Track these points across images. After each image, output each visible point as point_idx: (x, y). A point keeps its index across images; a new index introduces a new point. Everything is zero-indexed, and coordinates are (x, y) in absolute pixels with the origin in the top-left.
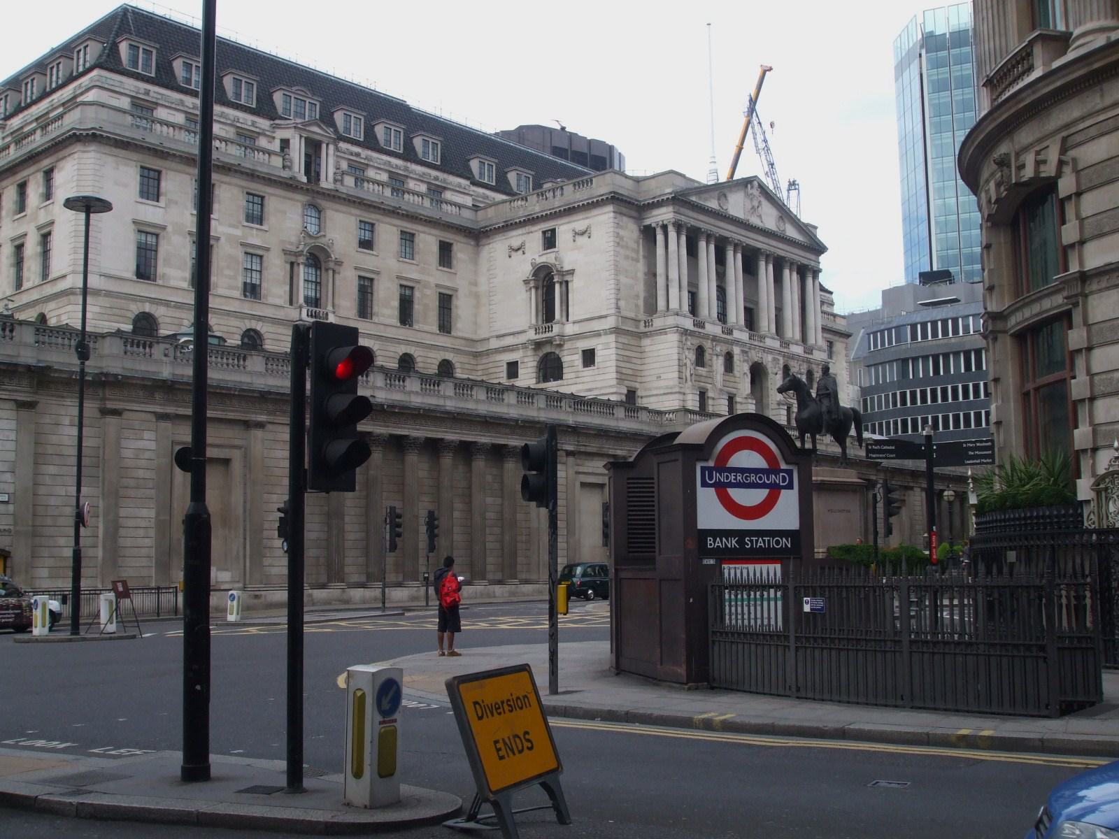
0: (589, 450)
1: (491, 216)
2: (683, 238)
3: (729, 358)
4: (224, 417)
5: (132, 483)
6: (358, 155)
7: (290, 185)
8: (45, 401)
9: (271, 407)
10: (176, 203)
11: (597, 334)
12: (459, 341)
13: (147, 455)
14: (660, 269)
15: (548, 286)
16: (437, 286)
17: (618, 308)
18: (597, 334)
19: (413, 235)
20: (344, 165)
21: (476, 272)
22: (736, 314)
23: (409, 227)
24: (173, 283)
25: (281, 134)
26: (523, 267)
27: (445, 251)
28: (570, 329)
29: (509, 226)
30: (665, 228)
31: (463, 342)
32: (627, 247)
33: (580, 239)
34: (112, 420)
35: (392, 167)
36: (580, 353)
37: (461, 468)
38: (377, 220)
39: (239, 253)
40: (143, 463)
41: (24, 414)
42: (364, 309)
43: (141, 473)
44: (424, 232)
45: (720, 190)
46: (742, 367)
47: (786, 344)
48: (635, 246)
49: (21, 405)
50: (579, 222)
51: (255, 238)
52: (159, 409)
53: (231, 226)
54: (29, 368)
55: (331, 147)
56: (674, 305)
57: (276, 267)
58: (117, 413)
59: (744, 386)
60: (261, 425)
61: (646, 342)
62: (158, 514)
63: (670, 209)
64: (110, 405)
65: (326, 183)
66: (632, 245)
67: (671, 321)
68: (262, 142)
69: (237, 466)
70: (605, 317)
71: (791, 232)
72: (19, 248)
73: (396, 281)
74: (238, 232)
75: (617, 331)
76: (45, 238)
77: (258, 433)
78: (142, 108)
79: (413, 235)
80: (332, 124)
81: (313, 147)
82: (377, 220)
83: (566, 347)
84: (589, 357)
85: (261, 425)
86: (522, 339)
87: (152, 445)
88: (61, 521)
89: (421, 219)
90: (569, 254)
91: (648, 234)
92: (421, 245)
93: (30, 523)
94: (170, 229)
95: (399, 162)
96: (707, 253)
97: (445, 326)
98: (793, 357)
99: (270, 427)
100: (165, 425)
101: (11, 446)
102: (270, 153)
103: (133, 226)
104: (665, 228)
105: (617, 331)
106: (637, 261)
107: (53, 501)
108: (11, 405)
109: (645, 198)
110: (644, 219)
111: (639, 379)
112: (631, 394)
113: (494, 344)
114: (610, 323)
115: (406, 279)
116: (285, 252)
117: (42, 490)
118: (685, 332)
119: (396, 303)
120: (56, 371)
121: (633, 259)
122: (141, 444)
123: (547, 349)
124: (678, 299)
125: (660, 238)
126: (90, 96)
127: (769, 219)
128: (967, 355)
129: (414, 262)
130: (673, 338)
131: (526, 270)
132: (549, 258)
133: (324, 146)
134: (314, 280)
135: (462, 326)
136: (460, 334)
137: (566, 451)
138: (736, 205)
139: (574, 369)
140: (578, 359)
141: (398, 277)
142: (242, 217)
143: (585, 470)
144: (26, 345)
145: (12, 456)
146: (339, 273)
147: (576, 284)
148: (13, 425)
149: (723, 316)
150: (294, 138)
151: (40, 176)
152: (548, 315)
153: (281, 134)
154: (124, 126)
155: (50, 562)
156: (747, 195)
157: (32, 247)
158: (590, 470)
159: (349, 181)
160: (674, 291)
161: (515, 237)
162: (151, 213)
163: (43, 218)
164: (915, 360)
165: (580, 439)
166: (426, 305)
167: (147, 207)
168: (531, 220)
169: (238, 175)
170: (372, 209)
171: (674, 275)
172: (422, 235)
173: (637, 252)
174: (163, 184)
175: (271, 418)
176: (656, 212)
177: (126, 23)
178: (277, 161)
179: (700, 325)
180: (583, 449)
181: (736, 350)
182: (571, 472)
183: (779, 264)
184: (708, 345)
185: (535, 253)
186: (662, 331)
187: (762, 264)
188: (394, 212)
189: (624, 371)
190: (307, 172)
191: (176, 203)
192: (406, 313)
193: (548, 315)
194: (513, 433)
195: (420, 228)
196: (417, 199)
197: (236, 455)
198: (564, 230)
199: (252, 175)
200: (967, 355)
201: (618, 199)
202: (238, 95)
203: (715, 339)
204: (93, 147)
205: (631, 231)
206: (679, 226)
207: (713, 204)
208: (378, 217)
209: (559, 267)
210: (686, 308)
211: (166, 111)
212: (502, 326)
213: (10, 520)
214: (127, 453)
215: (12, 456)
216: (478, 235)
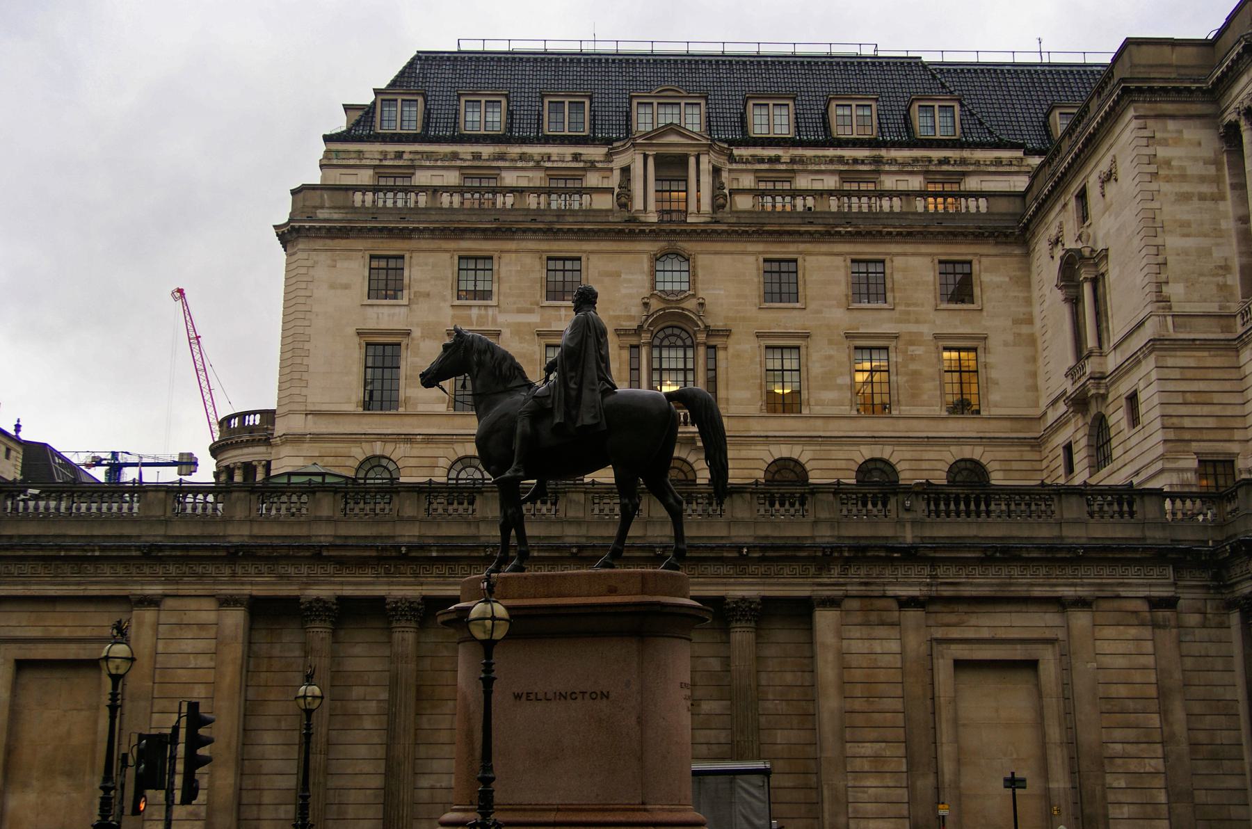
0: (968, 591)
4: (81, 593)
6: (777, 160)
12: (994, 425)
16: (937, 337)
17: (1162, 300)
18: (1135, 361)
21: (1028, 301)
24: (421, 408)
25: (619, 161)
31: (1007, 424)
32: (1183, 177)
33: (1111, 188)
35: (847, 163)
36: (1124, 402)
38: (800, 253)
44: (905, 254)
48: (1212, 170)
53: (520, 311)
66: (1194, 169)
70: (1140, 324)
73: (846, 343)
74: (534, 318)
82: (800, 253)
83: (1110, 399)
89: (890, 233)
92: (898, 276)
94: (417, 333)
99: (169, 603)
103: (357, 339)
106: (1219, 197)
110: (1223, 112)
111: (1238, 435)
121: (1202, 197)
129: (798, 305)
133: (692, 160)
134: (681, 366)
136: (995, 411)
137: (896, 598)
139: (1122, 437)
141: (848, 336)
142: (539, 294)
143: (970, 634)
146: (726, 348)
150: (633, 160)
158: (985, 634)
165: (940, 571)
167: (381, 310)
169: (529, 236)
170: (786, 238)
172: (899, 262)
173: (1218, 180)
175: (170, 589)
180: (947, 591)
189: (1187, 423)
194: (743, 573)
195: (894, 248)
201: (1139, 90)
208: (802, 247)
209: (1087, 252)
211: (429, 173)
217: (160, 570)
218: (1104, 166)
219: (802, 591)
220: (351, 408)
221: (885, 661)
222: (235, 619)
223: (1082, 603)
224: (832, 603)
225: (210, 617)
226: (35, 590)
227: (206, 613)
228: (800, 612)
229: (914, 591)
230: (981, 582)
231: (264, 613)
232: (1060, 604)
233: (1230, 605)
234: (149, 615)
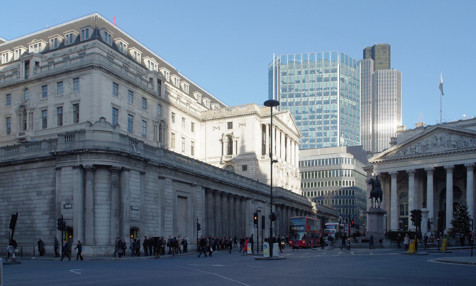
13: (170, 194)
34: (163, 180)
41: (142, 176)
43: (169, 201)
49: (142, 173)
54: (145, 159)
58: (163, 178)
60: (195, 186)
64: (163, 175)
69: (189, 199)
77: (195, 188)
85: (195, 186)
87: (171, 191)
88: (151, 218)
100: (175, 184)
101: (139, 188)
108: (138, 173)
115: (183, 135)
145: (139, 193)
197: (189, 196)
213: (139, 217)
214: (166, 193)
222: (204, 191)
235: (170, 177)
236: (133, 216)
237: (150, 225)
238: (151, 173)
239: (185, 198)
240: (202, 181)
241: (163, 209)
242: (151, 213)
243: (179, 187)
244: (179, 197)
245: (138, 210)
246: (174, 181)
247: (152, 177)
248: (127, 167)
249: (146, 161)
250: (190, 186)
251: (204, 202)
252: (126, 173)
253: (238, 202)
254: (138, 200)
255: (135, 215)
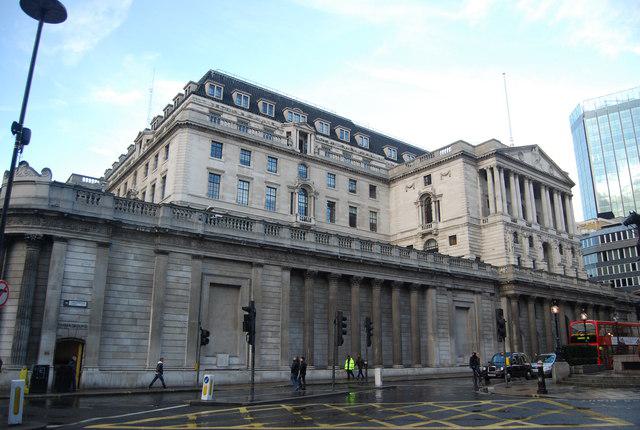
1: (391, 174)
2: (502, 175)
3: (531, 238)
5: (173, 298)
7: (291, 154)
8: (117, 243)
9: (267, 254)
10: (230, 160)
11: (457, 227)
13: (185, 281)
14: (490, 192)
15: (428, 205)
18: (457, 227)
19: (355, 182)
20: (320, 146)
22: (532, 216)
23: (354, 177)
25: (287, 129)
26: (414, 195)
27: (372, 189)
28: (441, 226)
29: (405, 176)
30: (492, 169)
34: (162, 258)
37: (386, 297)
39: (264, 187)
40: (180, 286)
41: (102, 250)
42: (332, 218)
43: (180, 292)
45: (520, 150)
46: (538, 245)
47: (559, 233)
49: (101, 245)
50: (444, 169)
51: (273, 179)
52: (193, 252)
55: (313, 136)
56: (499, 209)
57: (283, 195)
59: (540, 254)
60: (260, 265)
61: (484, 231)
62: (190, 319)
63: (494, 158)
64: (161, 248)
65: (311, 152)
67: (499, 218)
68: (277, 133)
71: (556, 174)
72: (154, 186)
74: (264, 176)
75: (469, 224)
76: (164, 178)
78: (215, 115)
79: (355, 182)
80: (313, 125)
81: (303, 135)
84: (453, 240)
85: (260, 265)
86: (415, 233)
88: (124, 321)
90: (439, 186)
91: (483, 174)
93: (100, 322)
95: (349, 146)
96: (514, 183)
97: (373, 227)
98: (563, 240)
100: (197, 262)
101: (92, 271)
102: (280, 137)
104: (492, 169)
105: (469, 224)
107: (119, 308)
109: (478, 154)
112: (478, 259)
113: (399, 237)
114: (465, 220)
116: (289, 187)
117: (111, 300)
118: (507, 224)
119: (348, 216)
120: (125, 224)
122: (181, 274)
123: (429, 237)
124: (501, 206)
125: (489, 174)
126: (190, 106)
127: (545, 167)
128: (621, 250)
130: (500, 227)
131: (417, 197)
132: (428, 189)
135: (381, 229)
138: (528, 159)
140: (447, 241)
144: (106, 208)
145: (92, 278)
147: (443, 202)
148: (94, 257)
149: (525, 216)
151: (164, 149)
152: (429, 219)
153: (287, 129)
154: (206, 121)
155: (115, 348)
156: (533, 154)
157: (159, 185)
159: (322, 153)
160: (499, 202)
161: (409, 181)
162: (216, 164)
163: (163, 169)
164: (610, 251)
166: (363, 218)
168: (418, 171)
171: (498, 193)
174: (224, 150)
176: (485, 162)
177: (212, 76)
178: (285, 142)
179: (514, 221)
181: (534, 235)
182: (451, 300)
183: (552, 191)
184: (519, 231)
185: (420, 187)
186: (494, 224)
187: (543, 191)
188: (345, 169)
190: (301, 148)
191: (230, 160)
192: (353, 222)
193: (429, 219)
194: (416, 276)
196: (358, 164)
197: (245, 284)
198: (435, 174)
199: (271, 147)
200: (621, 250)
202: (265, 111)
203: (523, 228)
204: (187, 130)
205: (473, 173)
206: (499, 168)
207: (516, 157)
210: (506, 211)
212: (403, 228)
213: (87, 319)
214: (171, 279)
215: (92, 278)
216: (388, 182)
217: (263, 254)
218: (444, 171)
219: (429, 283)
220: (204, 195)
221: (444, 306)
222: (287, 274)
223: (480, 293)
224: (434, 287)
225: (279, 273)
226: (220, 256)
227: (277, 271)
228: (423, 289)
229: (450, 286)
230: (462, 285)
231: (298, 274)
232: (474, 292)
233: (503, 296)
234: (260, 270)
235: (181, 253)
236: (67, 317)
237: (123, 335)
238: (134, 245)
239: (238, 287)
240: (281, 257)
241: (162, 307)
242: (128, 315)
243: (213, 268)
244: (213, 285)
245: (85, 307)
246: (195, 257)
247: (138, 251)
248: (59, 234)
249: (116, 228)
250: (249, 266)
251: (287, 297)
252: (57, 246)
253: (414, 295)
254: (87, 290)
255: (70, 315)
